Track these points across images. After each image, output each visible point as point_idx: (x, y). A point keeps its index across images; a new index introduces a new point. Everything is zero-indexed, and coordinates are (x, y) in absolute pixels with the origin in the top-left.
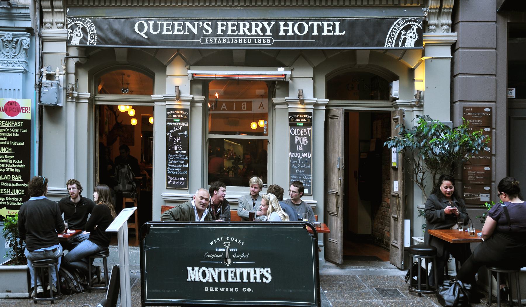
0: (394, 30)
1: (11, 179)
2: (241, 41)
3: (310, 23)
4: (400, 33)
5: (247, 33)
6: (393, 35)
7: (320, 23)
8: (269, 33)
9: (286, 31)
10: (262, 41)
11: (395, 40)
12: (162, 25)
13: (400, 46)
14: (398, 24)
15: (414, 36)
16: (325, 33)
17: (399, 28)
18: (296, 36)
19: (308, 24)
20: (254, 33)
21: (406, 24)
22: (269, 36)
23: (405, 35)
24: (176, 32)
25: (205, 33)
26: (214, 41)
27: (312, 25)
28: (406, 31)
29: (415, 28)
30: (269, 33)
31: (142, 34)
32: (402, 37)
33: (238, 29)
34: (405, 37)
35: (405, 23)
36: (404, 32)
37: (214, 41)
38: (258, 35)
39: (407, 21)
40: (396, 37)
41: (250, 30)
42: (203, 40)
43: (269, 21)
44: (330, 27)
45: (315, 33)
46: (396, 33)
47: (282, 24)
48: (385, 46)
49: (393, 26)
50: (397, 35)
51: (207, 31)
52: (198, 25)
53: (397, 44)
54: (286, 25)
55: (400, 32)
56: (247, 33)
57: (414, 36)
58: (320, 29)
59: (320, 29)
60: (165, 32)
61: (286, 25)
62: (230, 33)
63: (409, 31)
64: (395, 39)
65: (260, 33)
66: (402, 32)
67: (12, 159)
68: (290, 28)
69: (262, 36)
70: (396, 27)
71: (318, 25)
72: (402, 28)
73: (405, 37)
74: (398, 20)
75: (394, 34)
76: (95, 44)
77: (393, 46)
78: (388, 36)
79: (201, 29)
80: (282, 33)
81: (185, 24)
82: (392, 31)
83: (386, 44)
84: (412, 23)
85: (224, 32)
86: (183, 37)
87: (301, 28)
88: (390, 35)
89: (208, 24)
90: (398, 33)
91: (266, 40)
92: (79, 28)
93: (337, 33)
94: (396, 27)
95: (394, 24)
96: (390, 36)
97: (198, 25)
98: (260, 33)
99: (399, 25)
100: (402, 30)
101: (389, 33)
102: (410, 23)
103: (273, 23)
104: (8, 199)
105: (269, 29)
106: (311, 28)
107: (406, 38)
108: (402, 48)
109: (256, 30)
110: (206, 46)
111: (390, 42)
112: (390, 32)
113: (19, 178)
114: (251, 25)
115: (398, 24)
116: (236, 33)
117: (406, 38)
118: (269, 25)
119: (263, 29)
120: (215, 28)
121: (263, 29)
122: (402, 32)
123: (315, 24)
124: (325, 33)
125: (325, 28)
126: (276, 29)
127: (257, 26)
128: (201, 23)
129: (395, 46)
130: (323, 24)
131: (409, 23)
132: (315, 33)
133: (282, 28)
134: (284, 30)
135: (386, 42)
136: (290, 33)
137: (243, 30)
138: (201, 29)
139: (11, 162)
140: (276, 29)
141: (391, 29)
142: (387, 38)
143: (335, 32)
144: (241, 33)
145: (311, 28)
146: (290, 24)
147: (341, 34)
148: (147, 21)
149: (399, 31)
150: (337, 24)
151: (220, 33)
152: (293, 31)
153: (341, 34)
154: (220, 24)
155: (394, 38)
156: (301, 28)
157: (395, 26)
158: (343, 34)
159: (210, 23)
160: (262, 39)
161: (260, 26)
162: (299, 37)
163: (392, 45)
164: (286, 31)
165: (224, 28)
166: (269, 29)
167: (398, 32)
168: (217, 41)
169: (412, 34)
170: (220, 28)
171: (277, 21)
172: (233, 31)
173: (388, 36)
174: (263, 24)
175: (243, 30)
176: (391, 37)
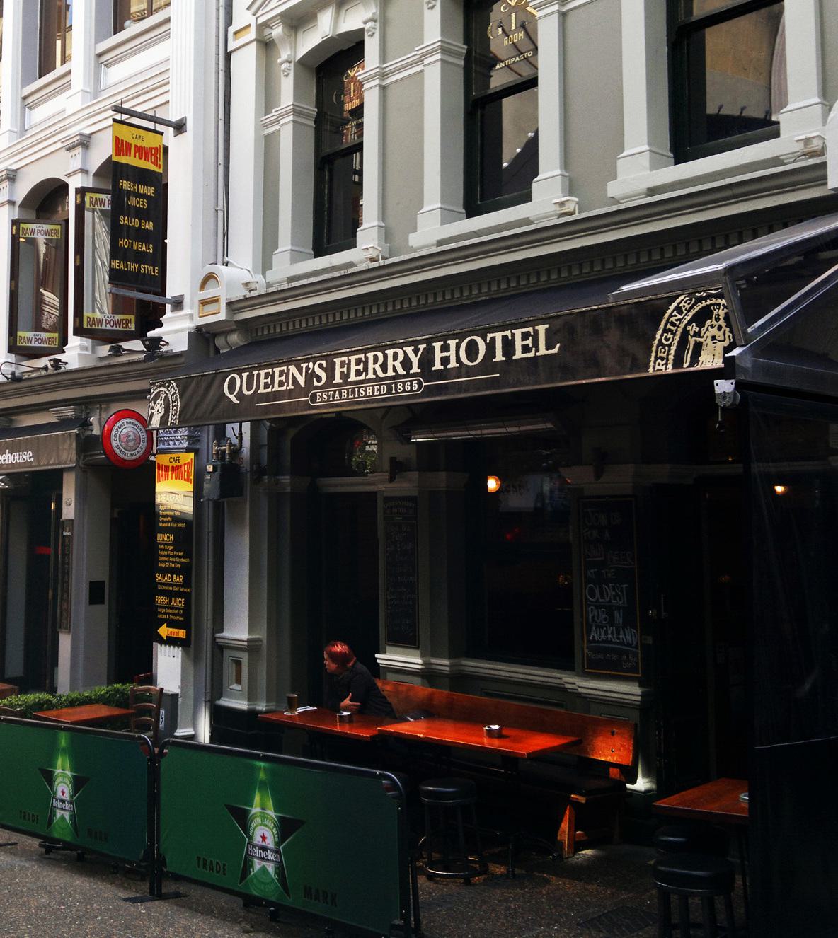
0: (669, 326)
1: (172, 581)
2: (369, 391)
3: (489, 336)
4: (685, 333)
5: (381, 374)
6: (667, 339)
7: (508, 333)
8: (415, 369)
9: (445, 361)
10: (404, 387)
11: (672, 352)
12: (259, 375)
13: (685, 365)
14: (679, 309)
15: (720, 335)
16: (519, 355)
17: (680, 320)
18: (463, 371)
19: (485, 340)
20: (390, 373)
21: (697, 308)
22: (415, 375)
23: (697, 334)
24: (276, 388)
25: (316, 383)
26: (329, 397)
27: (493, 339)
28: (701, 325)
29: (722, 313)
30: (415, 369)
31: (232, 397)
32: (692, 341)
33: (366, 369)
34: (698, 339)
35: (695, 304)
36: (694, 328)
37: (329, 397)
38: (397, 376)
39: (699, 300)
40: (676, 342)
41: (384, 367)
42: (314, 396)
43: (415, 344)
44: (527, 339)
45: (499, 357)
46: (674, 334)
47: (437, 346)
48: (651, 369)
49: (666, 316)
50: (677, 338)
51: (319, 379)
52: (307, 368)
53: (678, 361)
54: (445, 348)
55: (685, 329)
56: (381, 374)
57: (720, 335)
58: (508, 345)
59: (508, 345)
60: (262, 390)
61: (445, 348)
62: (353, 378)
63: (708, 323)
64: (674, 348)
65: (401, 372)
66: (689, 328)
67: (171, 550)
68: (452, 354)
69: (404, 376)
70: (672, 319)
71: (504, 338)
72: (688, 318)
73: (698, 339)
74: (678, 300)
75: (670, 336)
76: (177, 424)
77: (670, 366)
78: (656, 342)
79: (311, 376)
80: (438, 366)
81: (288, 370)
82: (665, 331)
83: (652, 364)
84: (714, 301)
85: (345, 376)
86: (290, 394)
87: (472, 350)
88: (660, 340)
89: (321, 366)
90: (679, 333)
91: (411, 386)
92: (161, 400)
93: (543, 351)
94: (672, 319)
95: (669, 312)
96: (660, 343)
97: (307, 368)
98: (401, 372)
99: (680, 312)
100: (689, 323)
101: (658, 337)
102: (709, 302)
103: (422, 347)
104: (169, 611)
105: (415, 360)
106: (491, 347)
107: (701, 343)
108: (692, 369)
109: (395, 366)
110: (318, 407)
111: (662, 359)
112: (660, 332)
113: (179, 579)
114: (385, 356)
115: (679, 309)
116: (362, 377)
117: (701, 343)
118: (416, 351)
119: (407, 363)
120: (330, 371)
121: (407, 363)
122: (689, 328)
123: (498, 336)
124: (519, 355)
125: (519, 343)
126: (426, 361)
127: (395, 357)
128: (311, 365)
129: (674, 366)
130: (513, 335)
131: (704, 303)
132: (499, 357)
133: (438, 355)
134: (442, 358)
135: (652, 359)
136: (453, 364)
137: (374, 369)
138: (311, 376)
139: (171, 553)
140: (426, 361)
141: (662, 326)
142: (654, 349)
143: (537, 350)
144: (371, 376)
145: (491, 347)
146: (452, 343)
147: (550, 352)
148: (240, 373)
149: (682, 326)
150: (542, 329)
151: (338, 380)
152: (458, 360)
153: (550, 352)
154: (338, 361)
155: (669, 346)
156: (472, 350)
157: (671, 316)
158: (555, 351)
159: (324, 363)
160: (404, 383)
161: (401, 357)
162: (469, 371)
163: (666, 364)
164: (445, 361)
165: (345, 369)
166: (415, 360)
167: (680, 330)
168: (334, 396)
169: (714, 331)
170: (338, 371)
171: (429, 342)
172: (358, 373)
173: (656, 342)
174: (405, 352)
175: (374, 369)
176: (664, 346)
